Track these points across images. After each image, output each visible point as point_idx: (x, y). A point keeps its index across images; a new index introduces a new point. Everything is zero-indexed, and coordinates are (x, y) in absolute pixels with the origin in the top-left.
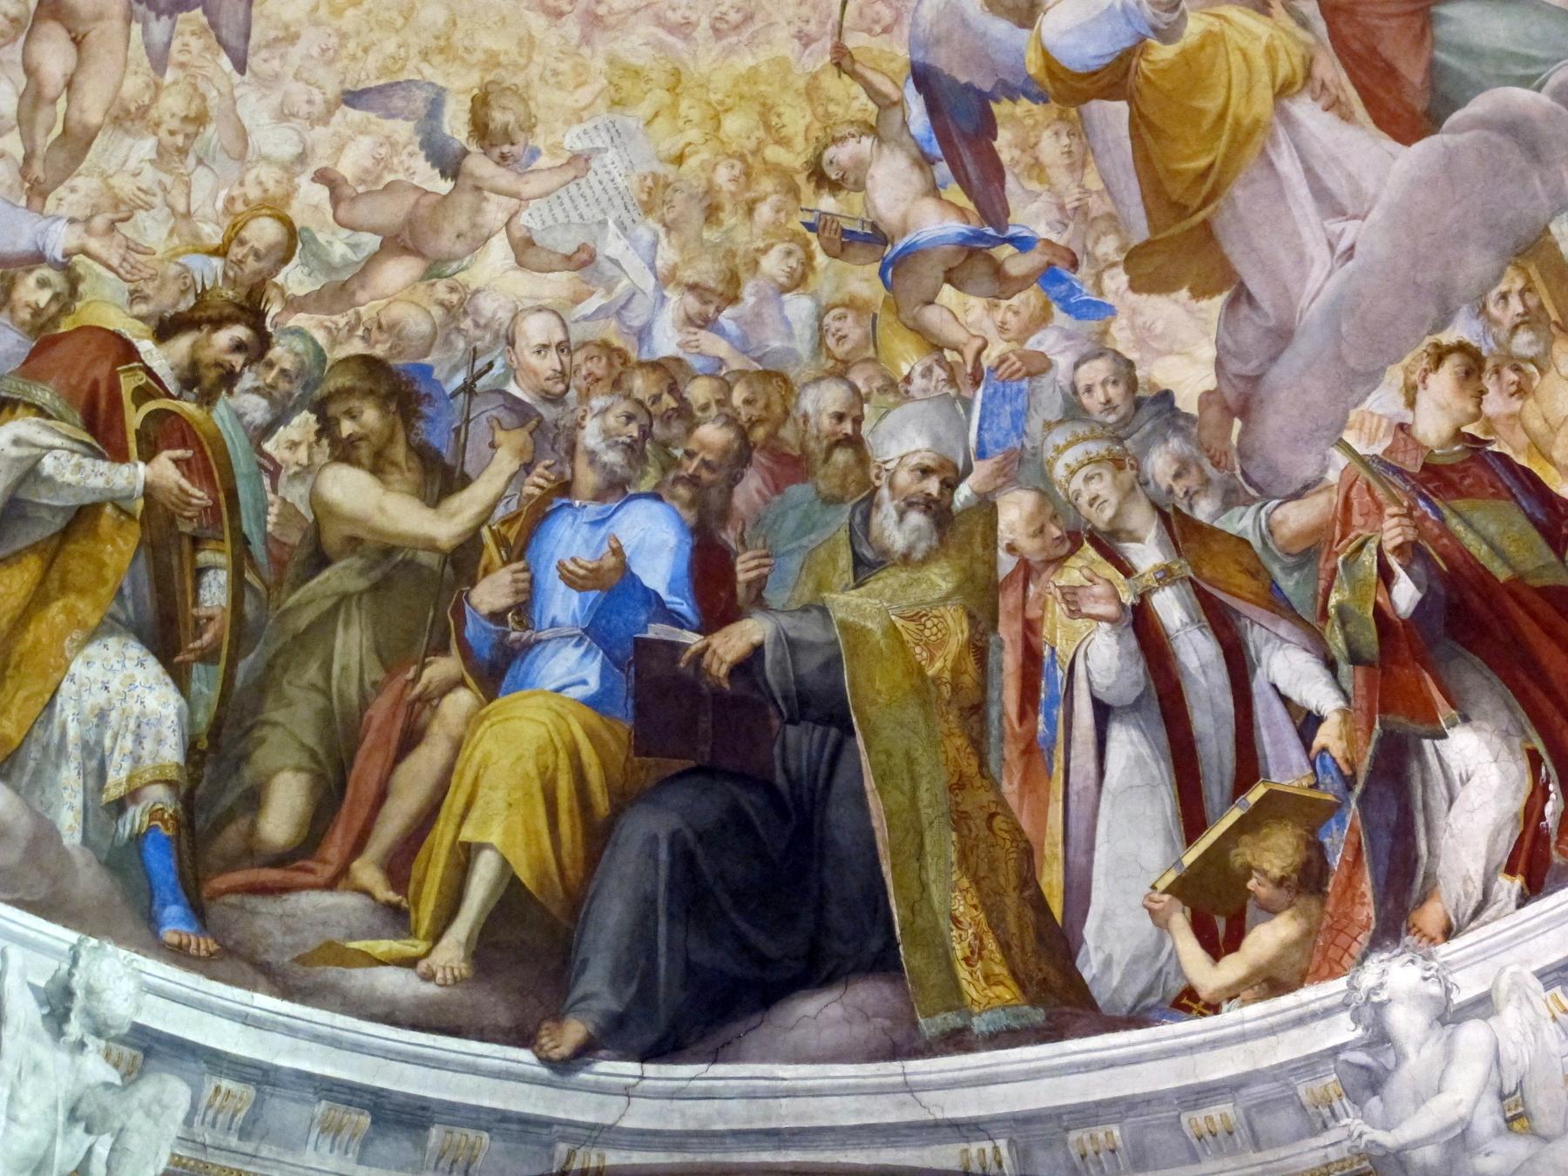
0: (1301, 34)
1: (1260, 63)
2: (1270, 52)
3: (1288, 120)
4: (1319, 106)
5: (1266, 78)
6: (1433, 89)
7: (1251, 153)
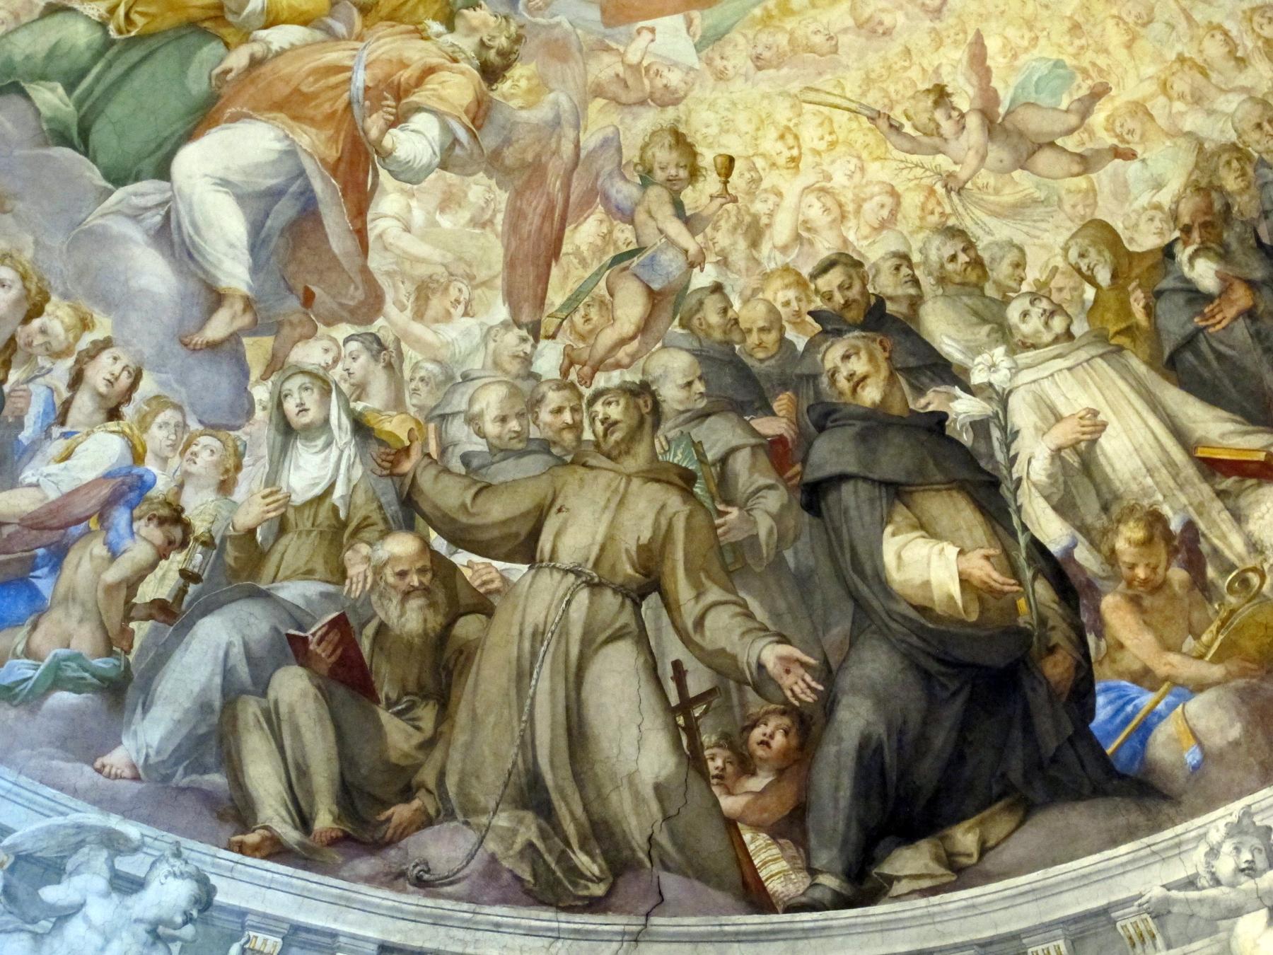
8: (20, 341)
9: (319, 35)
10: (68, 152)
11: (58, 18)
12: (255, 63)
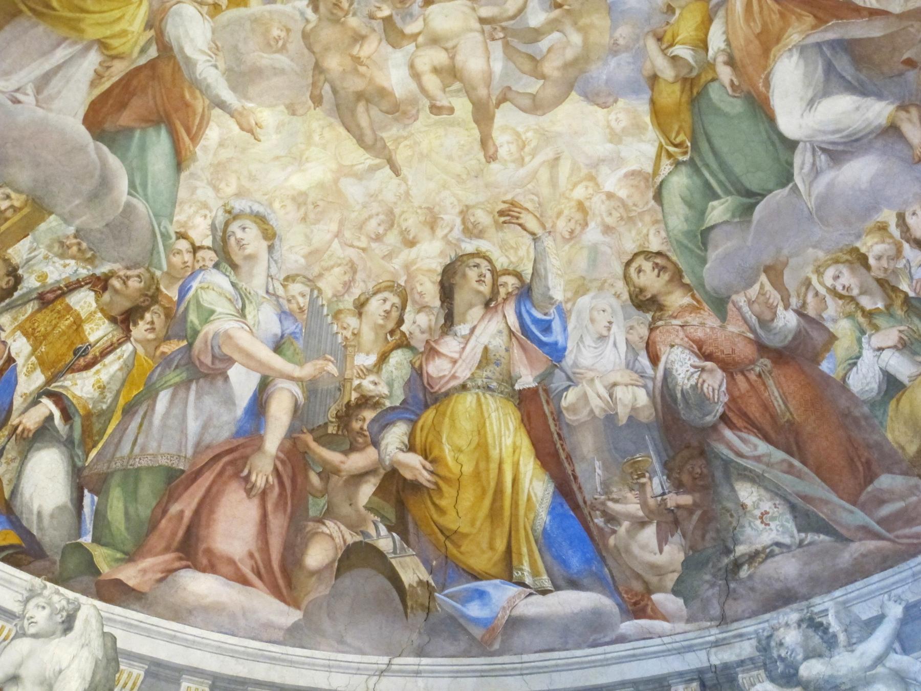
0: (137, 50)
1: (117, 28)
2: (124, 33)
3: (87, 49)
4: (97, 66)
5: (108, 33)
6: (118, 132)
7: (63, 32)
8: (881, 275)
9: (721, 13)
10: (758, 208)
11: (665, 193)
12: (731, 62)
